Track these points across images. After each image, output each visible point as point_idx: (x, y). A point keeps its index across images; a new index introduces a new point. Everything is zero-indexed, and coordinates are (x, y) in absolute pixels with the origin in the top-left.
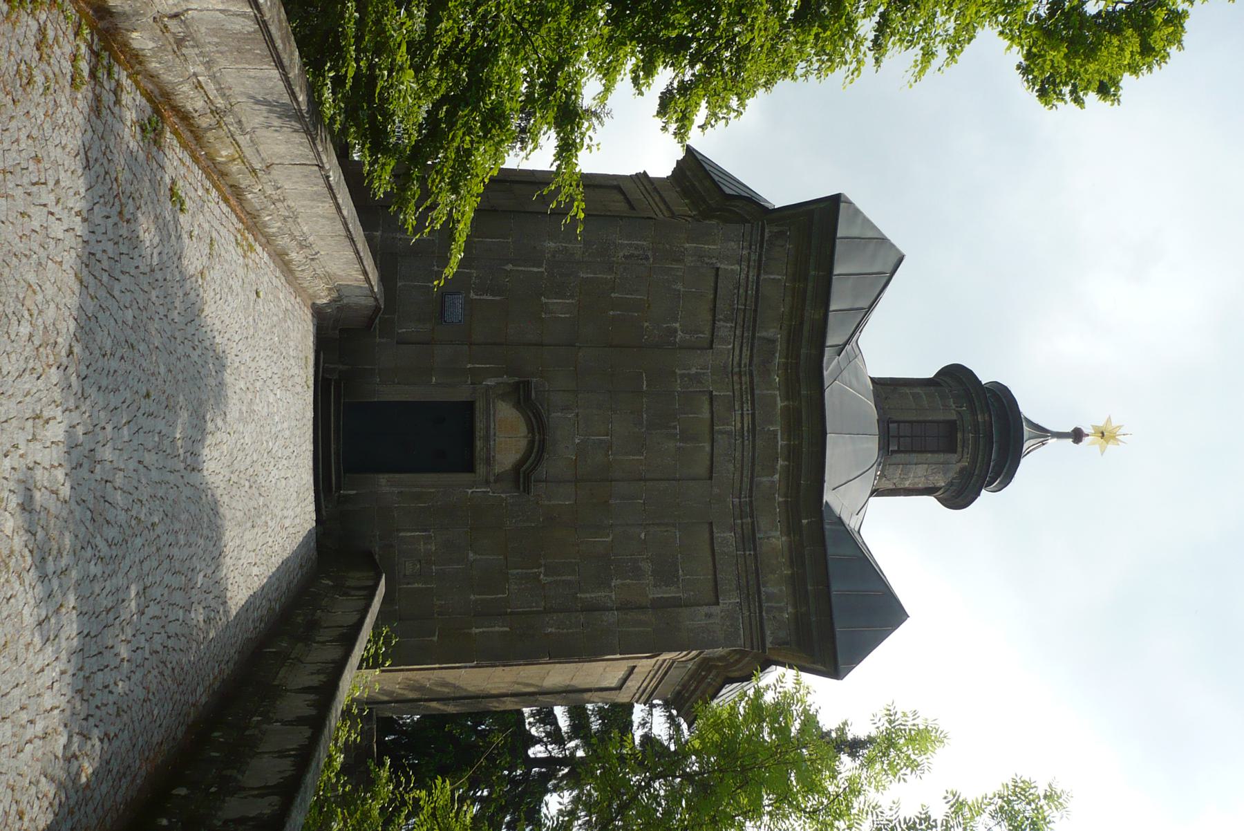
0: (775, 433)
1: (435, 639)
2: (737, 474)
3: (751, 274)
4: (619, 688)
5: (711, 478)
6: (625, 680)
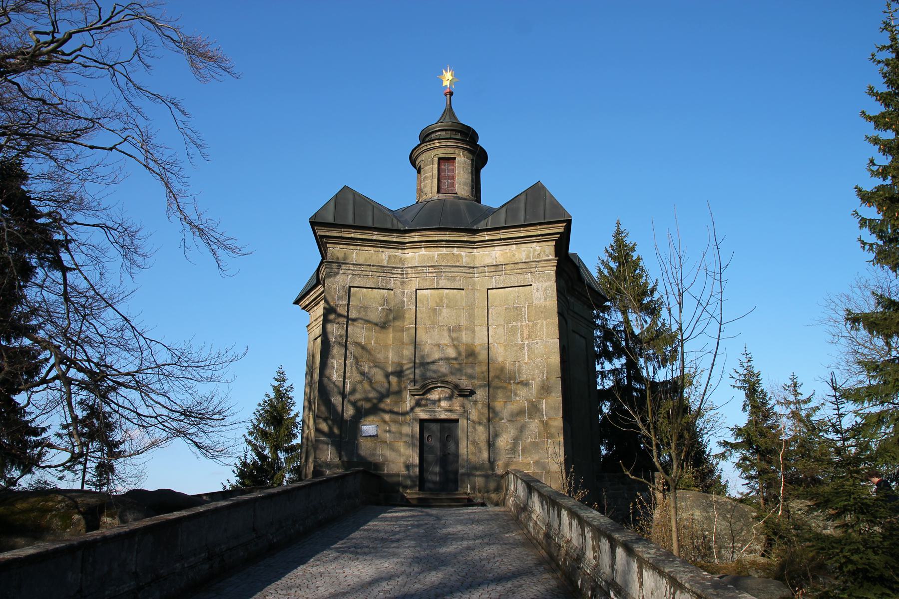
3: (353, 268)
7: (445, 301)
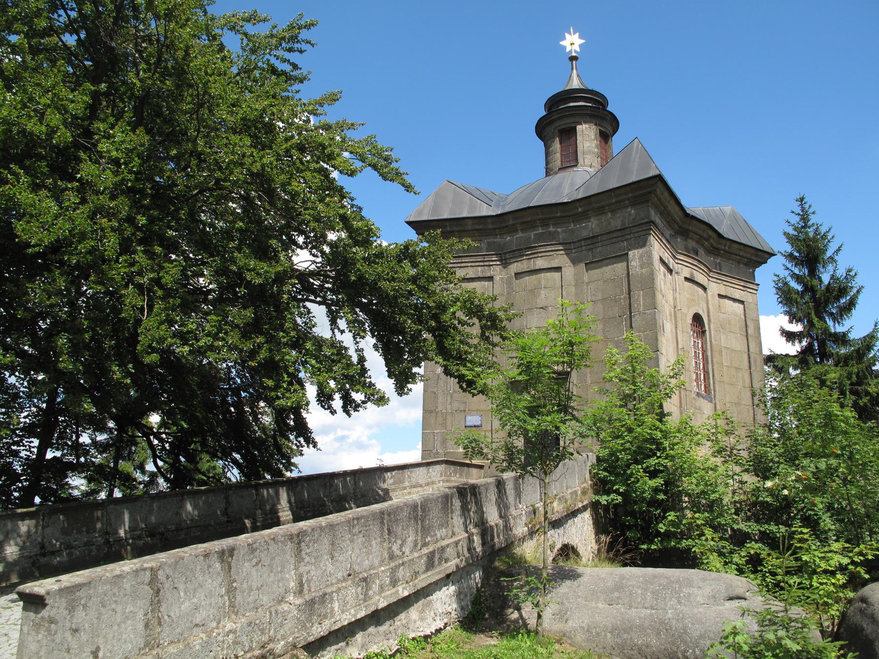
4: (742, 302)
6: (735, 300)
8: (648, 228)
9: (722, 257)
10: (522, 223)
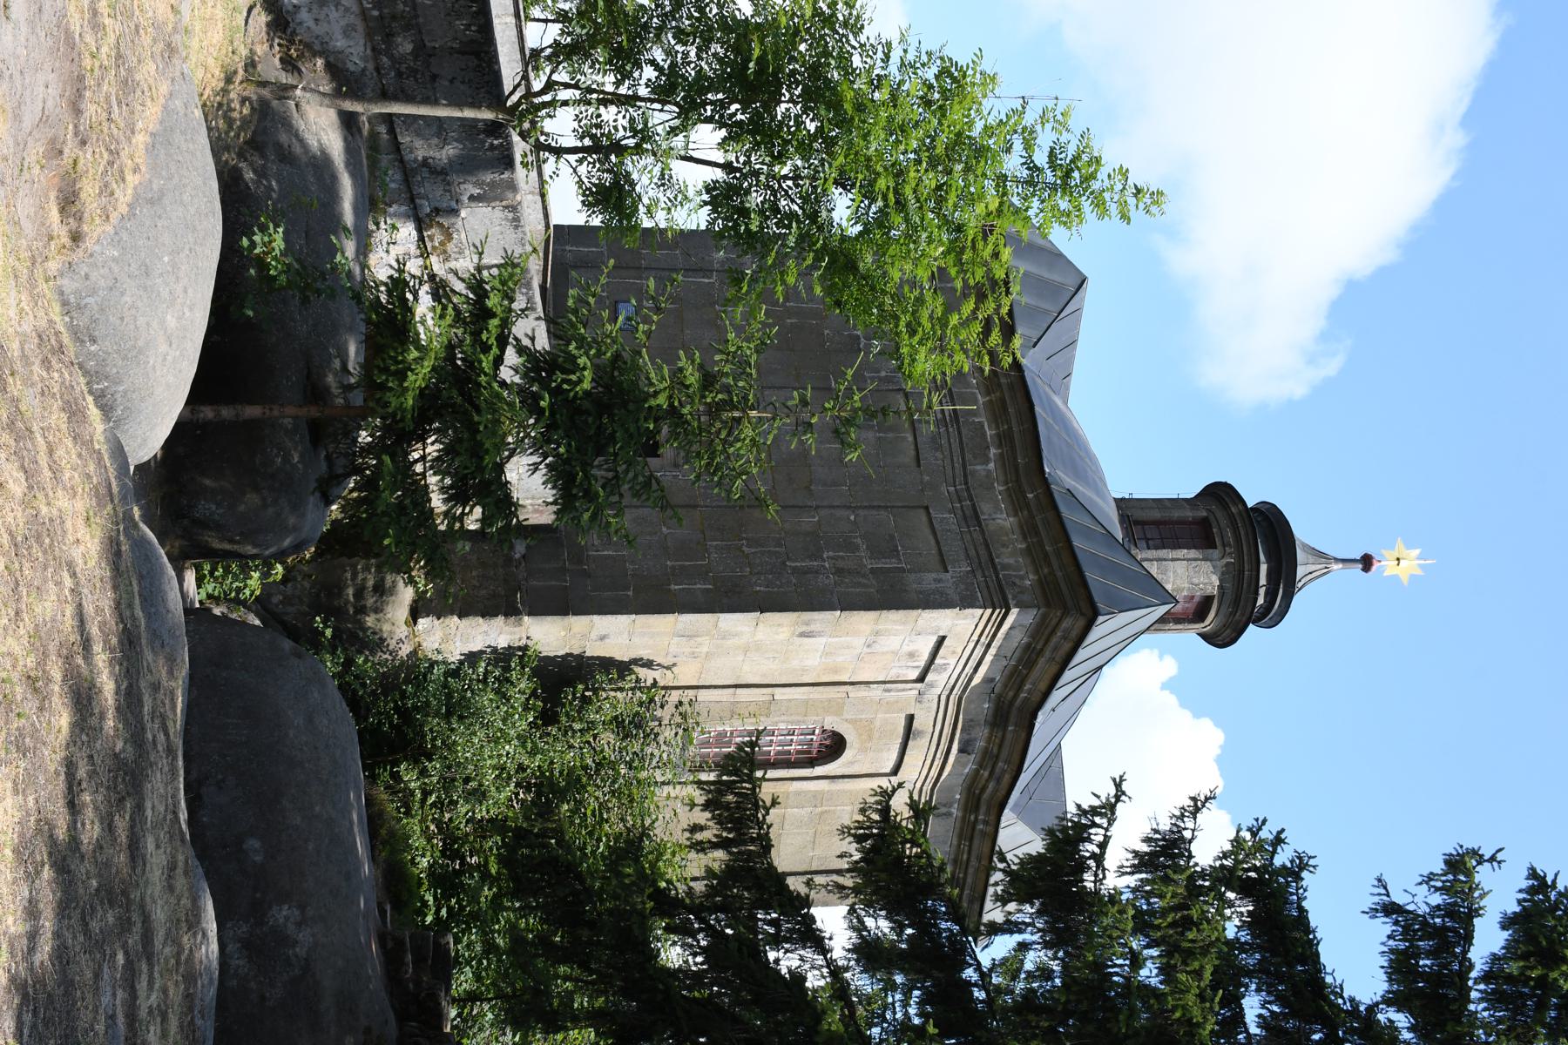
0: (981, 425)
1: (631, 593)
2: (948, 461)
5: (919, 465)
7: (890, 435)
8: (997, 604)
9: (964, 818)
10: (1003, 400)
